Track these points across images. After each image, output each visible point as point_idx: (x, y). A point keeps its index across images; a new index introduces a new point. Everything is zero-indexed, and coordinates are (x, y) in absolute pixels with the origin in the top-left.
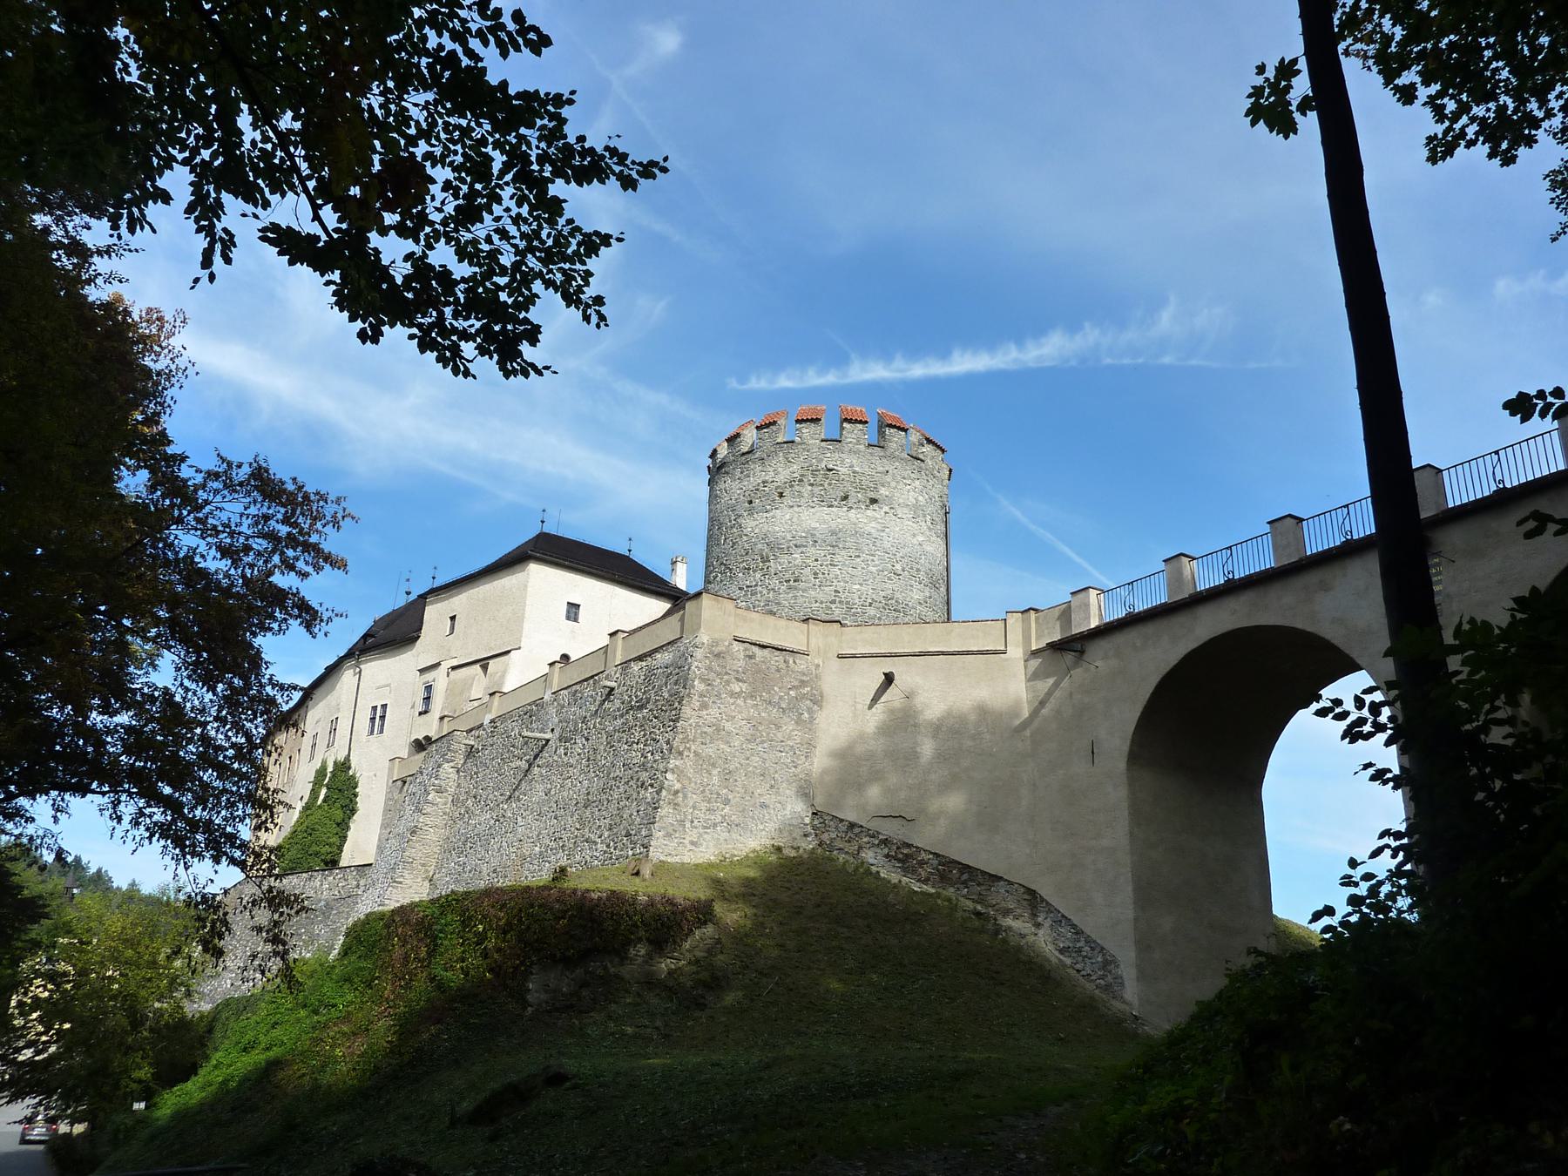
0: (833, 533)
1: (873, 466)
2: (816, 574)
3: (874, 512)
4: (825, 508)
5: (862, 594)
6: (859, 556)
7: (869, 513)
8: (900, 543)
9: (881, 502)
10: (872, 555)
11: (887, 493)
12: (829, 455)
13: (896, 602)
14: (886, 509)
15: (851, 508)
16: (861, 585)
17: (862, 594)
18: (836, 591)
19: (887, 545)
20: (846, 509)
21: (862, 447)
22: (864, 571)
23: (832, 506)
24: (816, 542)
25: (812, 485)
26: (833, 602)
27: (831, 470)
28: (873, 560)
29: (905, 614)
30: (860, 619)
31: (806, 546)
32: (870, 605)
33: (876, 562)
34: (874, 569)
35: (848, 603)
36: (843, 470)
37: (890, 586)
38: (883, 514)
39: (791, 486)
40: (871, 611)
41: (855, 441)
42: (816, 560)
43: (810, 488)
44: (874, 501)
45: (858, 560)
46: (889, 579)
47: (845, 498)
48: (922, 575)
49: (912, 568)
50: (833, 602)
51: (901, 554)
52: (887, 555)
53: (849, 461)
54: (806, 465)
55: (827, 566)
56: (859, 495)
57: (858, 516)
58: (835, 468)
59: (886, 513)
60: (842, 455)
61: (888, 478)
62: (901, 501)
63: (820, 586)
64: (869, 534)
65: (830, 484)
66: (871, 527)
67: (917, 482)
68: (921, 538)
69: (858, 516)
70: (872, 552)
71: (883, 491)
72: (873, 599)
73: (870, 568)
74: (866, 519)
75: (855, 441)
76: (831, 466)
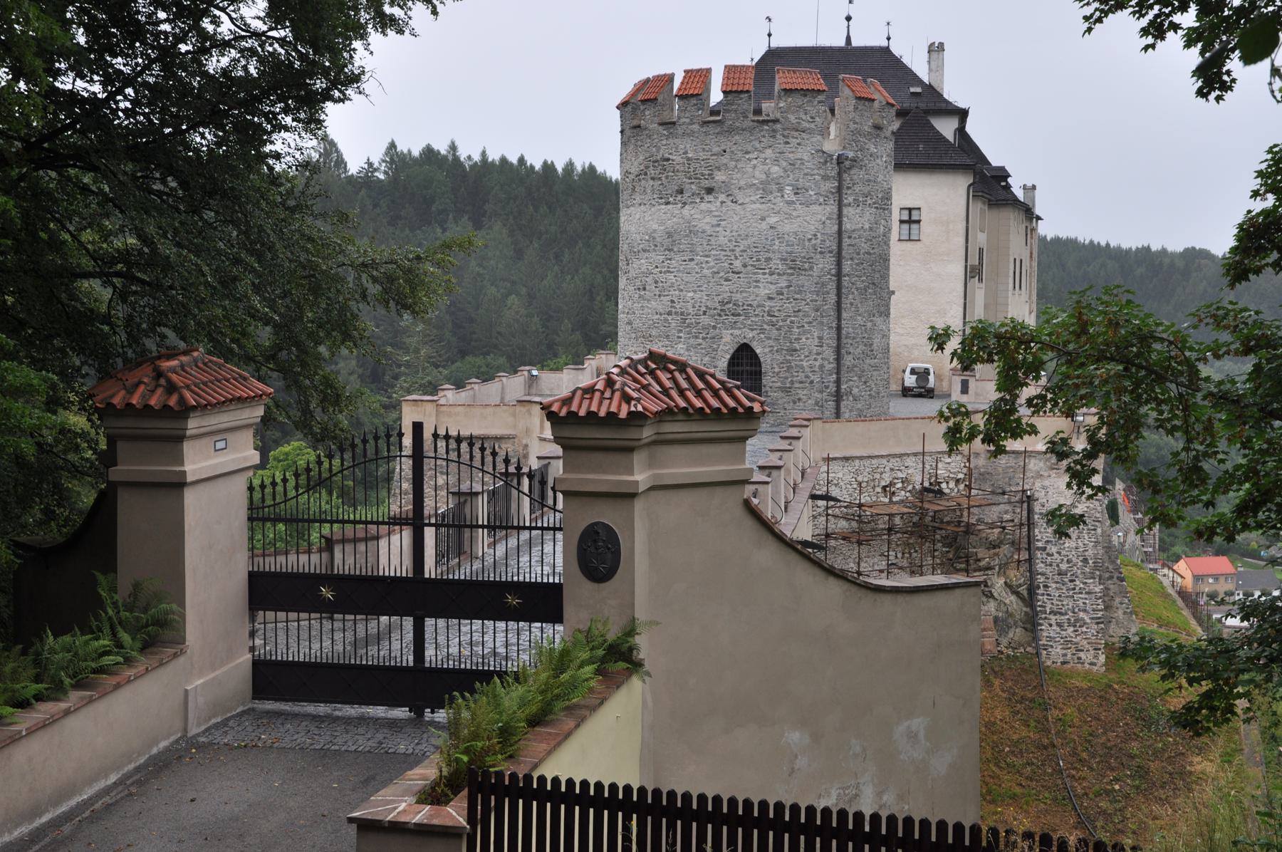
0: (670, 235)
1: (707, 148)
2: (656, 282)
3: (709, 205)
4: (663, 207)
5: (696, 302)
6: (693, 260)
7: (704, 206)
8: (739, 235)
9: (716, 189)
10: (707, 256)
11: (724, 178)
12: (664, 142)
13: (734, 305)
14: (722, 197)
15: (685, 204)
16: (695, 291)
17: (696, 302)
18: (673, 302)
19: (722, 240)
20: (680, 205)
21: (696, 127)
22: (697, 276)
23: (667, 203)
24: (656, 246)
25: (653, 179)
26: (669, 313)
27: (668, 160)
28: (707, 262)
29: (747, 317)
30: (694, 330)
31: (649, 251)
32: (705, 313)
33: (712, 264)
34: (705, 271)
35: (682, 314)
36: (677, 158)
37: (727, 288)
38: (718, 204)
39: (640, 180)
40: (705, 320)
41: (687, 120)
42: (657, 267)
43: (651, 182)
44: (710, 191)
45: (692, 263)
46: (727, 280)
47: (681, 192)
48: (777, 264)
49: (758, 260)
50: (669, 313)
51: (742, 248)
52: (723, 253)
53: (682, 146)
54: (648, 155)
55: (665, 272)
56: (693, 187)
57: (692, 212)
58: (670, 157)
59: (722, 202)
60: (676, 141)
61: (725, 159)
62: (742, 183)
63: (660, 296)
64: (704, 232)
65: (667, 177)
66: (705, 223)
67: (769, 151)
68: (773, 220)
69: (692, 212)
70: (707, 253)
71: (720, 176)
72: (707, 307)
73: (705, 271)
74: (701, 214)
75: (687, 120)
76: (667, 156)
